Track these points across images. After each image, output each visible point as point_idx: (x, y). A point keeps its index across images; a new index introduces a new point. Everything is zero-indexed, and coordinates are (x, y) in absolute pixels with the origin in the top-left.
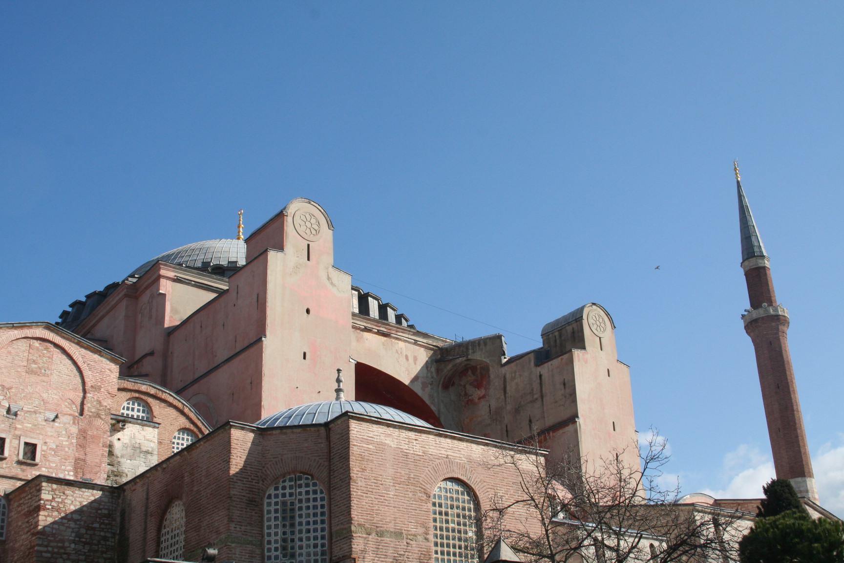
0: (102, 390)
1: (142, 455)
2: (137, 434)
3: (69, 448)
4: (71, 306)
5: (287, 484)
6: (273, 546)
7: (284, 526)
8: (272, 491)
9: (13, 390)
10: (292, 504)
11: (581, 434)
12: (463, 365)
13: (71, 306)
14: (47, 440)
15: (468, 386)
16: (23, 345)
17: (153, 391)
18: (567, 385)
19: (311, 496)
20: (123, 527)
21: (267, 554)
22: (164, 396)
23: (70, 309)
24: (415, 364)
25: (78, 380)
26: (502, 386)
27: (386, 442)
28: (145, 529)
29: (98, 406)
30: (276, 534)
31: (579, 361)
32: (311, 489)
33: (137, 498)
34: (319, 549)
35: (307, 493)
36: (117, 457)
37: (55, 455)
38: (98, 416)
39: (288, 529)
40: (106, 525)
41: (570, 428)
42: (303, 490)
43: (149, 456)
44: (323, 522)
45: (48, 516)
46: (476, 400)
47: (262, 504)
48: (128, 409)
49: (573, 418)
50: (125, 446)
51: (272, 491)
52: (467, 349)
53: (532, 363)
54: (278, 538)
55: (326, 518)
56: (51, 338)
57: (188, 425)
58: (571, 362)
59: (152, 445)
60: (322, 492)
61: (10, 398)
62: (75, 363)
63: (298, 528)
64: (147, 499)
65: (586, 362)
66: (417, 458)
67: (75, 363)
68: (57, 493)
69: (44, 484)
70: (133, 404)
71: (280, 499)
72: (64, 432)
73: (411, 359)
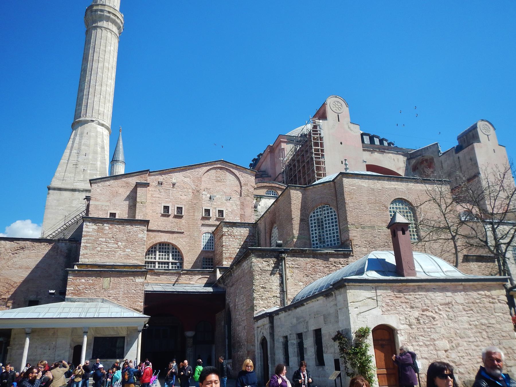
2: (267, 202)
3: (237, 210)
4: (252, 161)
5: (319, 210)
6: (315, 239)
7: (319, 229)
8: (312, 214)
10: (322, 219)
12: (421, 159)
13: (252, 161)
14: (228, 208)
16: (213, 171)
17: (277, 186)
19: (330, 214)
21: (312, 243)
24: (398, 162)
25: (238, 182)
27: (362, 184)
30: (316, 233)
32: (329, 211)
33: (261, 226)
34: (336, 238)
35: (328, 213)
38: (248, 196)
39: (321, 231)
40: (252, 239)
41: (476, 179)
42: (326, 212)
44: (336, 225)
45: (227, 238)
47: (308, 221)
51: (312, 214)
52: (422, 152)
53: (454, 153)
54: (317, 235)
55: (337, 223)
58: (473, 149)
60: (334, 212)
63: (325, 229)
66: (379, 190)
71: (316, 217)
72: (234, 204)
73: (396, 160)
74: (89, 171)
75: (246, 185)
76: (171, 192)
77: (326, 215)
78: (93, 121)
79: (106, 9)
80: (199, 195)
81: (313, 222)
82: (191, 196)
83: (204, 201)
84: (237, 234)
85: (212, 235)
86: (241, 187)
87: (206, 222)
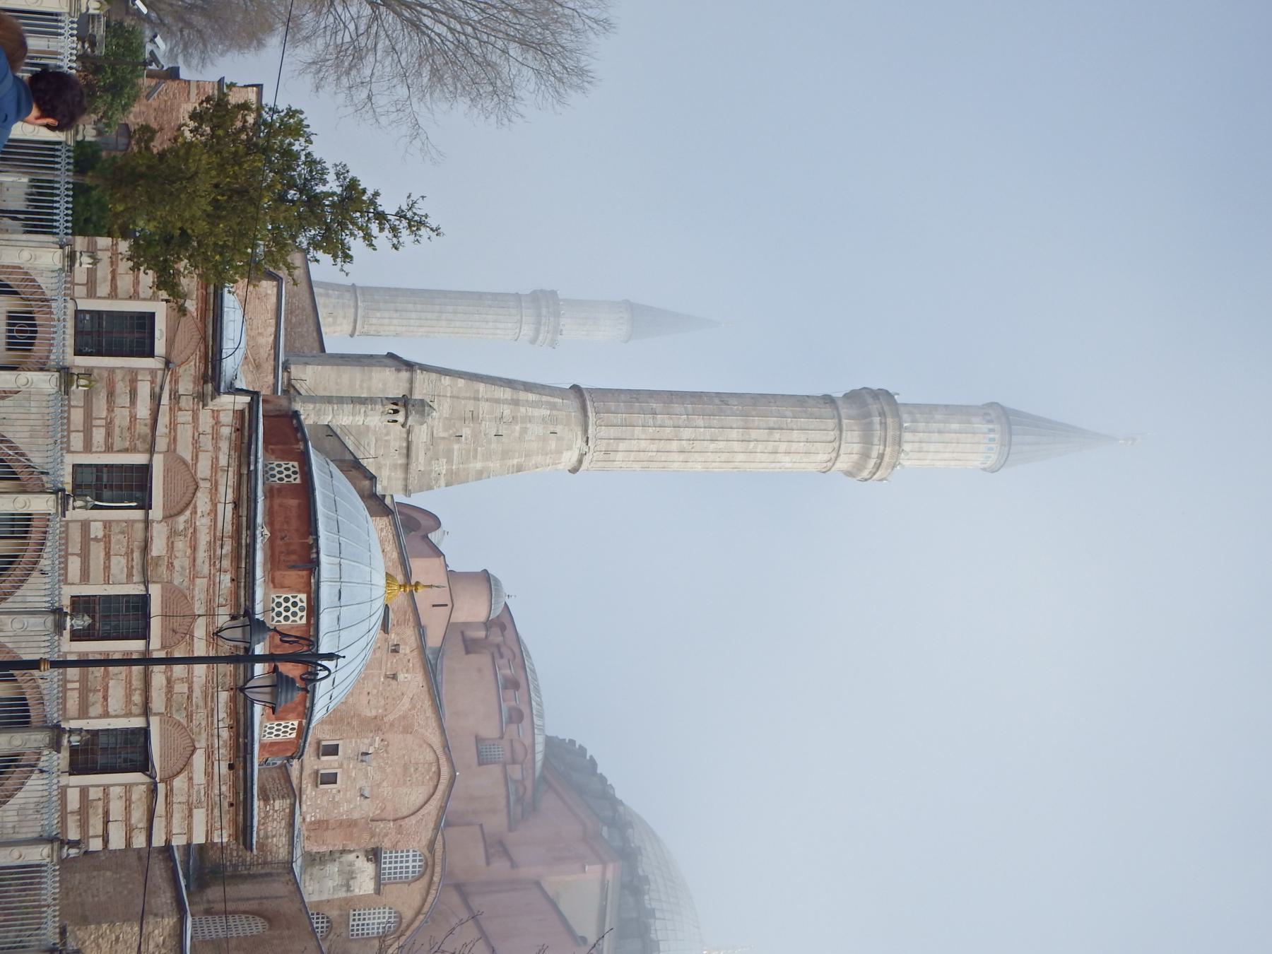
0: (399, 836)
1: (344, 881)
2: (366, 874)
4: (591, 757)
9: (385, 755)
16: (430, 757)
20: (253, 877)
23: (588, 758)
28: (248, 899)
29: (382, 834)
33: (279, 888)
36: (339, 858)
37: (329, 802)
38: (373, 836)
43: (344, 889)
48: (414, 856)
50: (351, 864)
56: (441, 781)
57: (405, 922)
59: (357, 890)
61: (377, 753)
62: (421, 807)
64: (277, 898)
67: (421, 807)
68: (282, 813)
69: (288, 801)
70: (420, 861)
72: (352, 806)
74: (456, 447)
76: (376, 672)
78: (587, 442)
79: (888, 450)
80: (371, 731)
82: (369, 715)
83: (356, 742)
84: (270, 829)
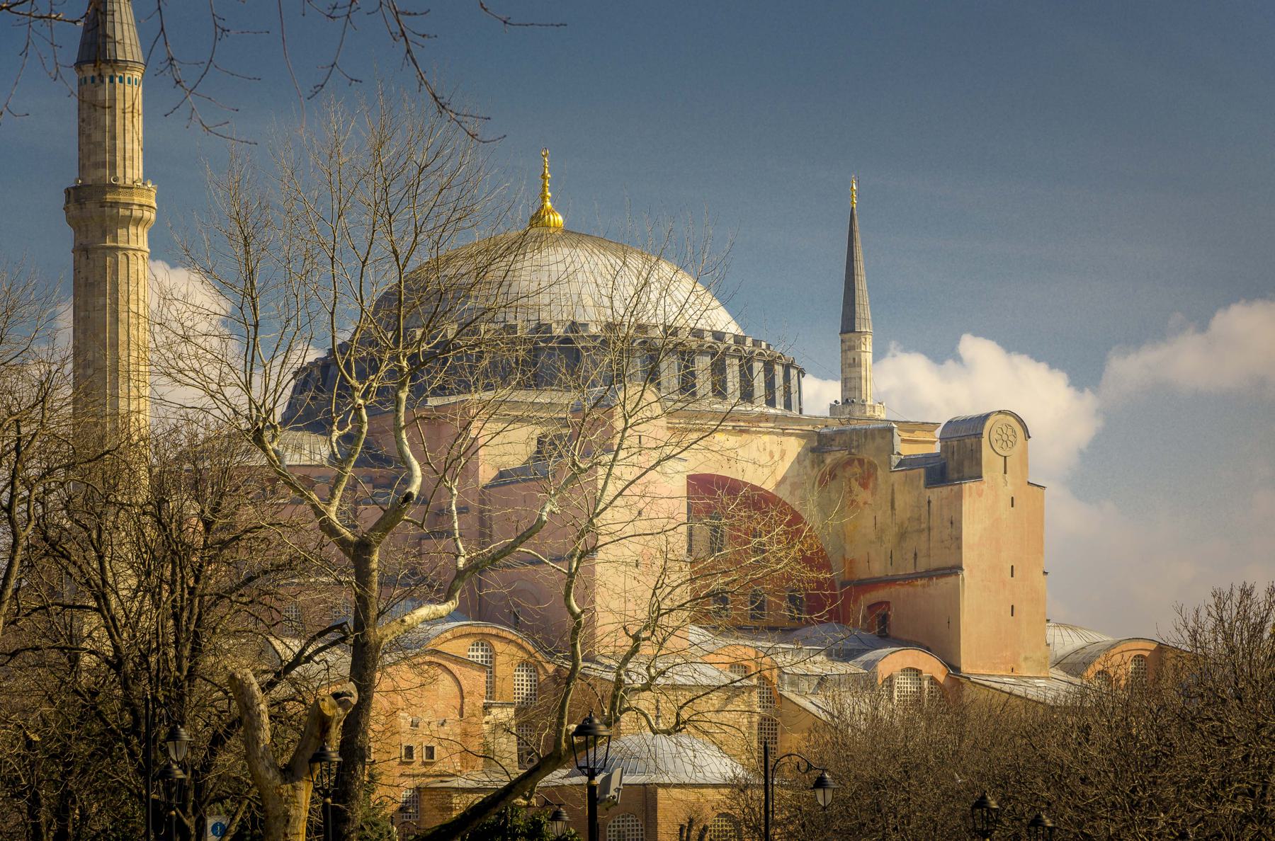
10: (624, 832)
11: (963, 590)
15: (853, 480)
17: (494, 632)
18: (954, 525)
22: (504, 634)
25: (456, 689)
26: (890, 498)
31: (970, 496)
41: (951, 579)
42: (630, 824)
46: (861, 504)
49: (956, 569)
51: (611, 823)
58: (959, 497)
60: (641, 825)
65: (980, 495)
75: (471, 693)
77: (630, 828)
81: (612, 834)
85: (416, 793)
86: (462, 697)
87: (408, 770)
